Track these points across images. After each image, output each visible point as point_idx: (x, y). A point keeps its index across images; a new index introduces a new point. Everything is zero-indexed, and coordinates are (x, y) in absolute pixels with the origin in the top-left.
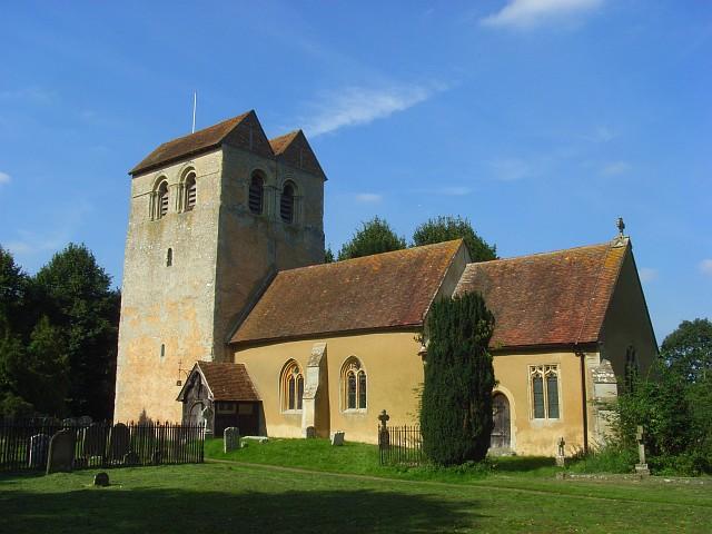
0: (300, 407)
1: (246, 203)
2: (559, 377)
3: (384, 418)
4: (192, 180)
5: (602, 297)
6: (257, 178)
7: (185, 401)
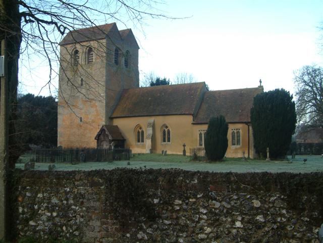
0: (143, 141)
1: (114, 62)
2: (241, 132)
3: (184, 146)
7: (98, 140)
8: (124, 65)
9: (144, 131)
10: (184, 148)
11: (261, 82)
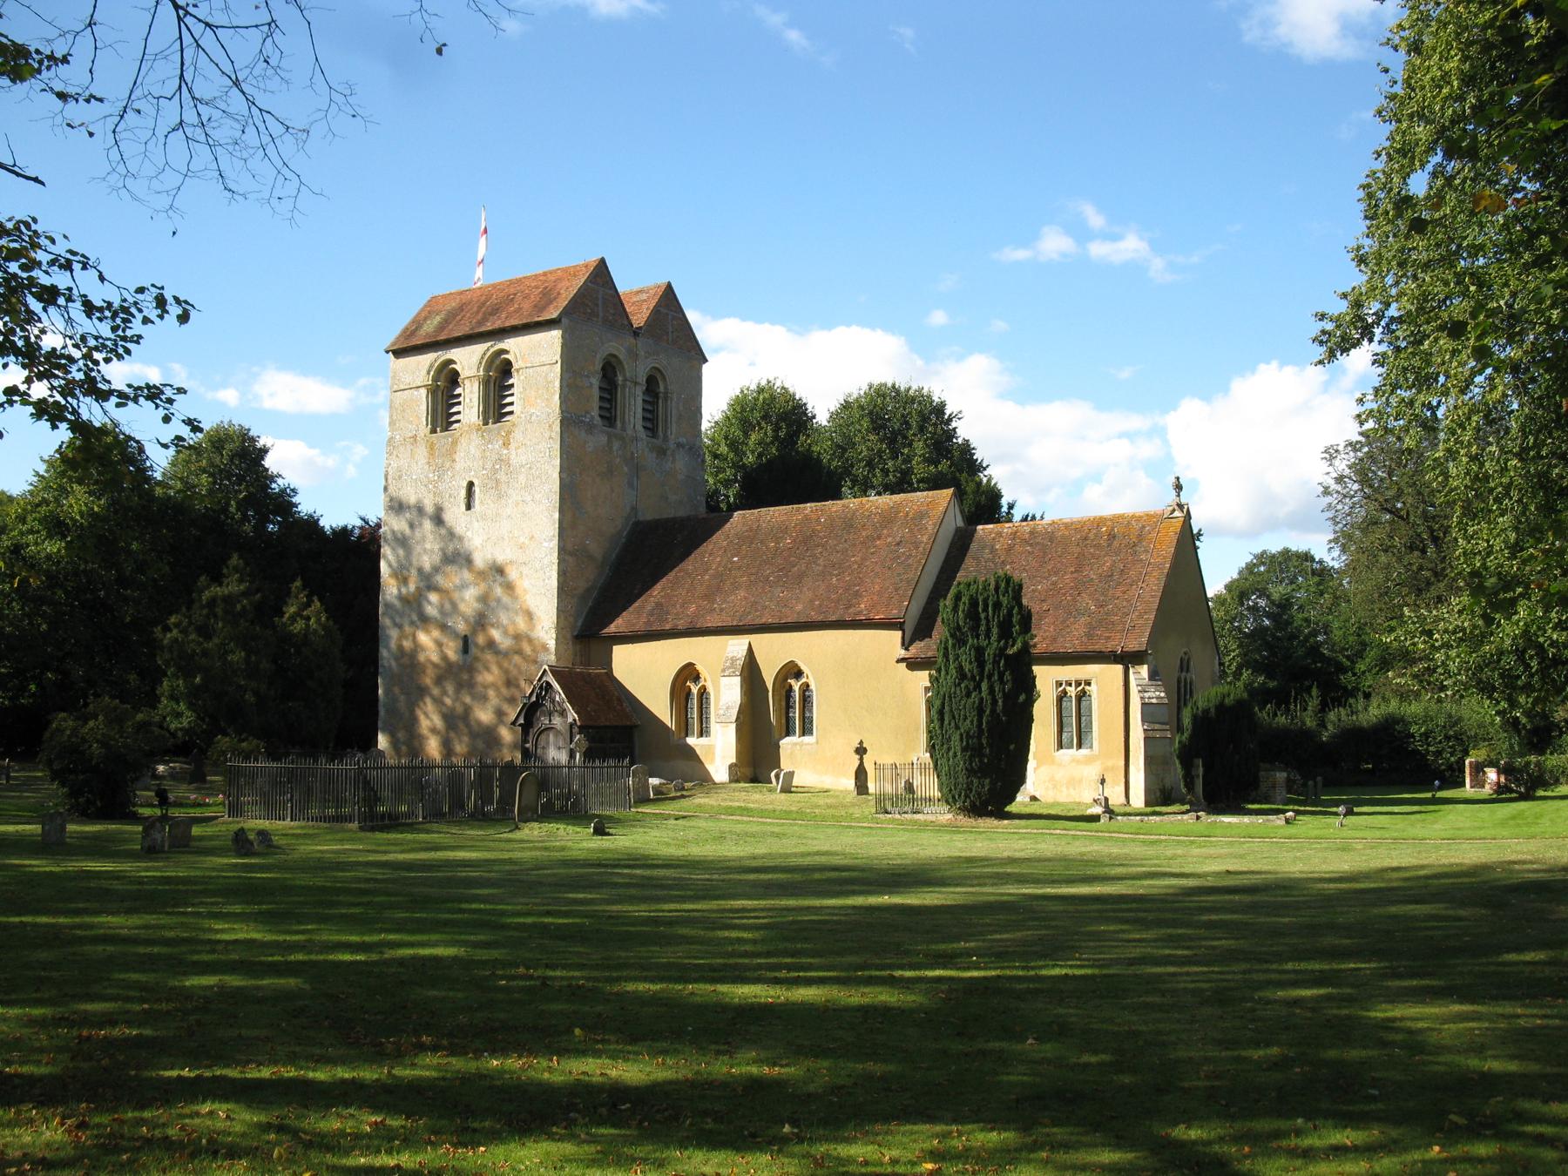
1: (595, 413)
2: (1094, 696)
3: (861, 751)
4: (506, 369)
5: (1150, 589)
6: (609, 370)
8: (639, 427)
9: (710, 689)
10: (861, 759)
11: (1178, 487)
